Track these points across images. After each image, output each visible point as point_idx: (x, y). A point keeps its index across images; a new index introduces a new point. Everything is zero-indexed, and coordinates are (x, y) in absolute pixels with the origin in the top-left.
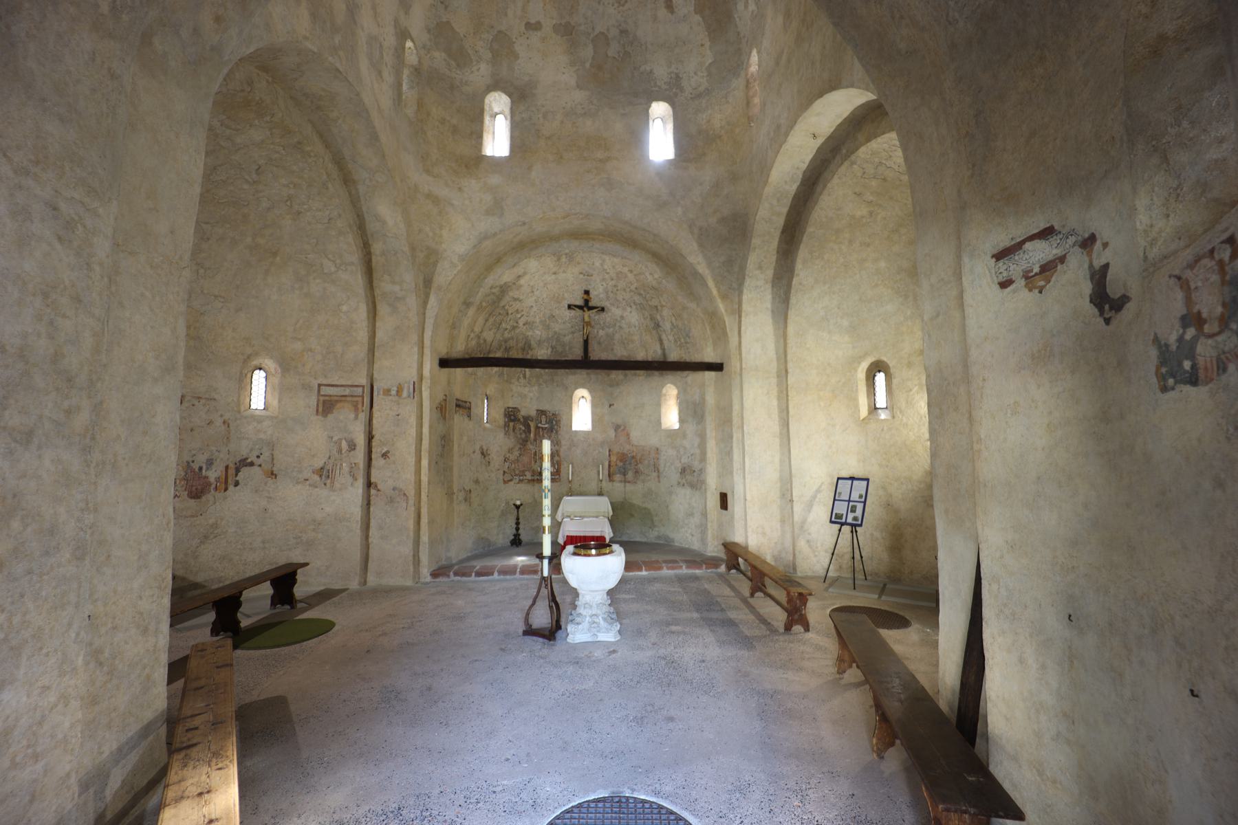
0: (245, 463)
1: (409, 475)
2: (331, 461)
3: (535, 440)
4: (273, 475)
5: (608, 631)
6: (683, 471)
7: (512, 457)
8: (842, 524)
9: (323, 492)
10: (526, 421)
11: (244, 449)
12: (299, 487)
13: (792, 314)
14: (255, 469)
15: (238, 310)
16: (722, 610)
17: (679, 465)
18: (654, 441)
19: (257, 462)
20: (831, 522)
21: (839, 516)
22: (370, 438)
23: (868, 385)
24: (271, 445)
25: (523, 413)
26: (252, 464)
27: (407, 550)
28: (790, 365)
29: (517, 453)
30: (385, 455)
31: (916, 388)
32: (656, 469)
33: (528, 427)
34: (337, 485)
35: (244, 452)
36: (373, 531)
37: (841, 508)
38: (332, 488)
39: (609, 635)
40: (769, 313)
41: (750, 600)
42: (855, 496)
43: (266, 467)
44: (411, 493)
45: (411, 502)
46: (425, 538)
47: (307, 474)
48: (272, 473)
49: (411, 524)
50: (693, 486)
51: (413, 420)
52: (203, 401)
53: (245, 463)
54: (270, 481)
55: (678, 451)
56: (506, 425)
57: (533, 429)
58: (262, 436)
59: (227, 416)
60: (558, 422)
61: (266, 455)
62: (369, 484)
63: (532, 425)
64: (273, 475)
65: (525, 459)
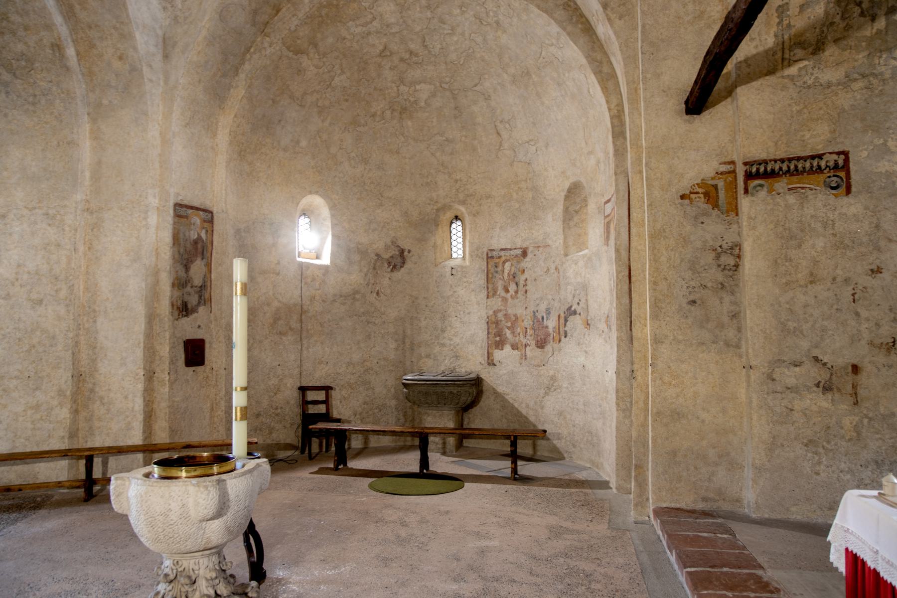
0: (572, 312)
15: (547, 146)
26: (575, 313)
52: (541, 249)
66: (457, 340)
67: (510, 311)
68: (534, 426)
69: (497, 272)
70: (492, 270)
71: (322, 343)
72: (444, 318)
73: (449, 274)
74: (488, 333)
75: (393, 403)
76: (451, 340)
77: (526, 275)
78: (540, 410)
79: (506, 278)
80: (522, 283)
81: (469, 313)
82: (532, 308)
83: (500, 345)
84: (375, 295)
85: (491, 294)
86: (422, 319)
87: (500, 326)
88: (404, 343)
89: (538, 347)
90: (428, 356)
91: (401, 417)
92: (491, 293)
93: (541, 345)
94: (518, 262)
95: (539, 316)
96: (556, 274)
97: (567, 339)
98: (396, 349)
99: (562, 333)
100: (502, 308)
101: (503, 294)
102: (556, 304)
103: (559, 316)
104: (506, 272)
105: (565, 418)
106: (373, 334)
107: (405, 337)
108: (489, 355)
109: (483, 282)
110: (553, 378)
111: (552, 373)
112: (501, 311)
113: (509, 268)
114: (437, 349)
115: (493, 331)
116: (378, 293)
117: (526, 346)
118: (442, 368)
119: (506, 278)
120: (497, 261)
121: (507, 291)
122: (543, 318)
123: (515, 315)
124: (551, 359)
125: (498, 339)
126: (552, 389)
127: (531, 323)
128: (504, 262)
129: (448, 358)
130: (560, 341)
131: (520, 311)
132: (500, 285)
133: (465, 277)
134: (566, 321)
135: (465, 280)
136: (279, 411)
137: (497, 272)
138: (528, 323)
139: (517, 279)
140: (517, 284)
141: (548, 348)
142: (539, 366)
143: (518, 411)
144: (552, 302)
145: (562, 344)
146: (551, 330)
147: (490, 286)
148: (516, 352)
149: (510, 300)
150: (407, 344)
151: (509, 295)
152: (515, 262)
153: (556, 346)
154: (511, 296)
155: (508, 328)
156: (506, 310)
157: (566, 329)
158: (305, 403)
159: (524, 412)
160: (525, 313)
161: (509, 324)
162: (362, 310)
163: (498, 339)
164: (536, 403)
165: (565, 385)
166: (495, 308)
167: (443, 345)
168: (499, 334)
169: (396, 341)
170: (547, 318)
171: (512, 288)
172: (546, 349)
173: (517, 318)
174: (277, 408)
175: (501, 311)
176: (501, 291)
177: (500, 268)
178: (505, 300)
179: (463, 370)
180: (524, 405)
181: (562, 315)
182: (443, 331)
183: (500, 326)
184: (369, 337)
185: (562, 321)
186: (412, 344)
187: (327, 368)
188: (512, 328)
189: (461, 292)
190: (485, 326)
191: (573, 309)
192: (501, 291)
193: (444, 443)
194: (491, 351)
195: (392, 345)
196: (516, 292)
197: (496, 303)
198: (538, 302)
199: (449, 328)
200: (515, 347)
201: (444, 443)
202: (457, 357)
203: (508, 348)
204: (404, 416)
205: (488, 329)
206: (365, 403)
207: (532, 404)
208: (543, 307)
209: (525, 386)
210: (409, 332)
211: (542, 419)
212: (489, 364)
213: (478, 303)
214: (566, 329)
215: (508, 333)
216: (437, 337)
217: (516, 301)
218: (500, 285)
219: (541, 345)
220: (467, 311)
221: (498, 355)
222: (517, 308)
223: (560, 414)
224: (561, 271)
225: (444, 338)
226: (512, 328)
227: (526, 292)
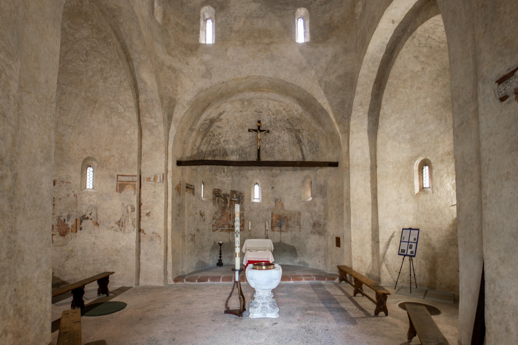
0: (84, 218)
1: (161, 226)
2: (124, 217)
3: (230, 207)
4: (97, 224)
5: (272, 312)
6: (314, 225)
7: (217, 217)
8: (405, 256)
9: (120, 234)
10: (225, 196)
11: (84, 210)
12: (109, 231)
13: (380, 131)
14: (89, 221)
16: (337, 303)
17: (312, 222)
18: (297, 207)
19: (90, 217)
20: (399, 254)
21: (403, 251)
22: (140, 205)
23: (419, 174)
24: (96, 208)
25: (223, 192)
26: (87, 218)
27: (160, 266)
28: (378, 162)
29: (220, 215)
30: (148, 214)
31: (445, 175)
32: (299, 224)
33: (226, 200)
34: (127, 230)
35: (84, 212)
36: (142, 256)
37: (404, 246)
38: (124, 232)
39: (273, 315)
40: (366, 132)
41: (354, 298)
42: (412, 239)
43: (94, 220)
44: (162, 235)
45: (163, 240)
46: (170, 260)
47: (113, 224)
48: (97, 224)
49: (162, 252)
50: (320, 234)
51: (163, 195)
53: (84, 218)
55: (311, 214)
56: (214, 199)
57: (229, 201)
58: (92, 203)
60: (243, 197)
61: (94, 213)
62: (140, 230)
63: (228, 199)
64: (97, 224)
65: (225, 218)
82: (58, 214)
95: (62, 219)
97: (82, 231)
103: (76, 220)
122: (65, 220)
127: (57, 223)
130: (76, 232)
134: (81, 222)
144: (72, 212)
146: (70, 226)
153: (73, 234)
170: (68, 220)
181: (79, 219)
185: (79, 222)
191: (86, 216)
198: (61, 211)
208: (65, 215)
224: (79, 197)
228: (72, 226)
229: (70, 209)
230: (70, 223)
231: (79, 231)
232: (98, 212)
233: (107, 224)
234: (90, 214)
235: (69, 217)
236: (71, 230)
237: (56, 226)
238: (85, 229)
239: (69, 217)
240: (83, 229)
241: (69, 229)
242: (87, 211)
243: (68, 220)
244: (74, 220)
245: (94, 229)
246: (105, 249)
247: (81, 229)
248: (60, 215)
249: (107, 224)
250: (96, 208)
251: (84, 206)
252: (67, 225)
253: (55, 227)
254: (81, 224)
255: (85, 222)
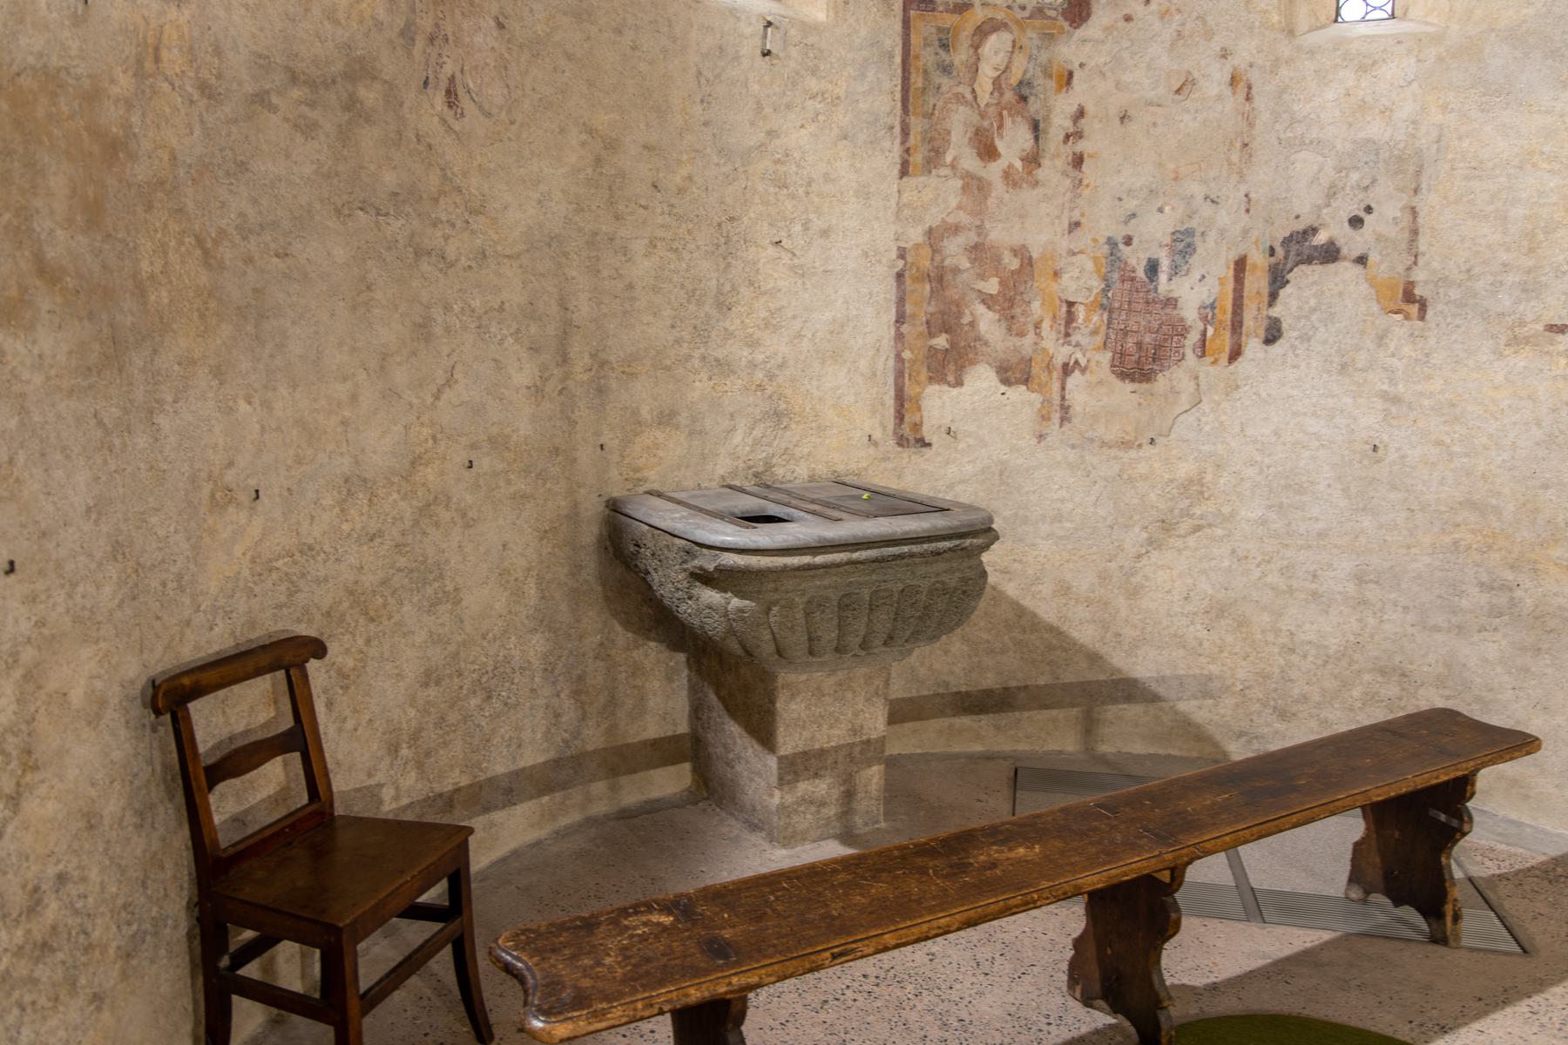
0: (1305, 249)
4: (1411, 300)
11: (1300, 189)
12: (1521, 360)
14: (1345, 271)
19: (1353, 242)
24: (1411, 169)
26: (1330, 254)
35: (1303, 205)
48: (1409, 297)
53: (1305, 249)
54: (1399, 328)
58: (1375, 129)
59: (1245, 51)
64: (1411, 300)
66: (777, 346)
67: (998, 234)
68: (1094, 658)
69: (946, 69)
70: (927, 57)
71: (218, 372)
72: (726, 247)
73: (750, 48)
74: (900, 319)
75: (537, 645)
76: (753, 344)
77: (1081, 93)
78: (1121, 602)
79: (985, 97)
80: (1060, 122)
81: (825, 233)
82: (1105, 225)
83: (949, 364)
84: (439, 100)
85: (917, 158)
86: (639, 246)
87: (953, 293)
88: (564, 359)
89: (1123, 376)
90: (666, 418)
91: (567, 704)
92: (918, 154)
93: (1138, 367)
94: (1049, 38)
95: (1136, 259)
96: (1231, 103)
97: (1277, 349)
98: (537, 391)
99: (1252, 320)
100: (964, 218)
101: (970, 162)
102: (1227, 217)
103: (1240, 265)
104: (987, 72)
105: (1242, 623)
106: (437, 313)
107: (567, 328)
108: (903, 403)
109: (883, 101)
110: (1195, 488)
111: (1185, 469)
112: (956, 229)
113: (1000, 59)
114: (700, 387)
115: (922, 307)
116: (450, 93)
117: (1067, 370)
118: (722, 466)
119: (985, 97)
120: (949, 20)
121: (988, 152)
122: (1153, 268)
123: (1020, 252)
124: (1190, 419)
125: (941, 341)
126: (1185, 526)
127: (1097, 285)
128: (982, 32)
129: (742, 424)
130: (1235, 354)
131: (1042, 236)
132: (959, 124)
133: (814, 71)
134: (1278, 279)
135: (813, 84)
136: (52, 910)
137: (946, 69)
138: (1080, 280)
139: (1034, 106)
140: (1035, 127)
141: (1177, 378)
142: (1125, 445)
143: (1020, 611)
144: (1207, 210)
145: (1241, 365)
146: (1190, 313)
147: (917, 124)
148: (1018, 393)
149: (999, 187)
150: (581, 365)
151: (994, 171)
152: (1031, 37)
153: (1213, 372)
154: (1007, 175)
155: (988, 301)
156: (980, 229)
157: (1276, 311)
158: (194, 777)
159: (1047, 612)
160: (1064, 243)
161: (992, 286)
162: (389, 179)
163: (941, 341)
164: (1104, 577)
165: (1251, 511)
166: (934, 218)
167: (723, 367)
168: (947, 321)
169: (534, 349)
170: (1175, 271)
171: (1014, 141)
172: (1161, 382)
173: (1028, 262)
174: (34, 905)
175: (956, 229)
176: (960, 150)
177: (961, 56)
178: (976, 187)
179: (802, 471)
180: (1046, 589)
181: (1258, 259)
182: (724, 307)
183: (953, 293)
184: (423, 330)
185: (1257, 282)
186: (601, 364)
187: (255, 529)
188: (1007, 304)
189: (798, 137)
190: (885, 290)
191: (1321, 238)
192: (960, 150)
193: (849, 795)
194: (910, 389)
195: (522, 374)
196: (1033, 160)
197: (939, 197)
198: (1131, 204)
199: (746, 292)
200: (1014, 373)
201: (849, 795)
202: (778, 415)
203: (982, 379)
204: (576, 694)
205: (901, 302)
206: (429, 678)
207: (1084, 582)
208: (1155, 232)
209: (1059, 518)
210: (583, 308)
211: (1129, 633)
212: (902, 441)
213: (864, 193)
214: (1276, 311)
215: (987, 322)
216: (701, 333)
217: (1028, 195)
218: (959, 124)
219: (1138, 367)
220: (818, 224)
221: (939, 405)
222: (1031, 222)
223: (1218, 610)
225: (729, 335)
226: (1007, 304)
227: (1078, 161)
228: (1208, 312)
229: (1196, 189)
230: (1194, 292)
231: (1253, 346)
232: (1429, 201)
233: (1505, 301)
234: (1356, 222)
235: (1184, 245)
236: (1193, 337)
237: (1090, 308)
238: (1306, 338)
239: (1184, 245)
240: (1290, 333)
241: (1181, 331)
242: (1332, 193)
243: (1175, 271)
244: (1222, 269)
245: (1381, 339)
246: (1470, 504)
247: (1273, 335)
248: (1119, 233)
249: (1505, 301)
250: (1411, 169)
251: (1306, 163)
252: (1171, 302)
253: (1081, 313)
254: (1273, 297)
255: (1305, 282)
